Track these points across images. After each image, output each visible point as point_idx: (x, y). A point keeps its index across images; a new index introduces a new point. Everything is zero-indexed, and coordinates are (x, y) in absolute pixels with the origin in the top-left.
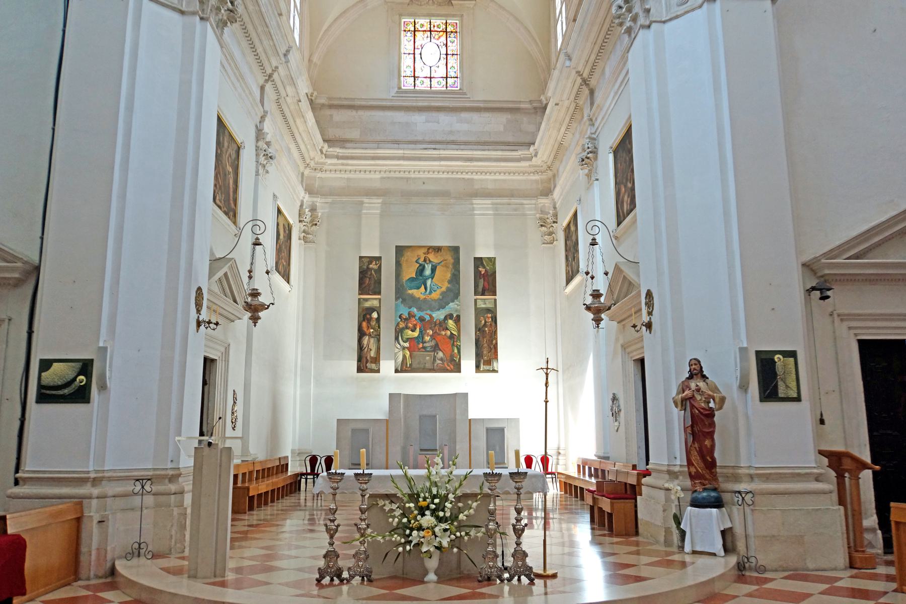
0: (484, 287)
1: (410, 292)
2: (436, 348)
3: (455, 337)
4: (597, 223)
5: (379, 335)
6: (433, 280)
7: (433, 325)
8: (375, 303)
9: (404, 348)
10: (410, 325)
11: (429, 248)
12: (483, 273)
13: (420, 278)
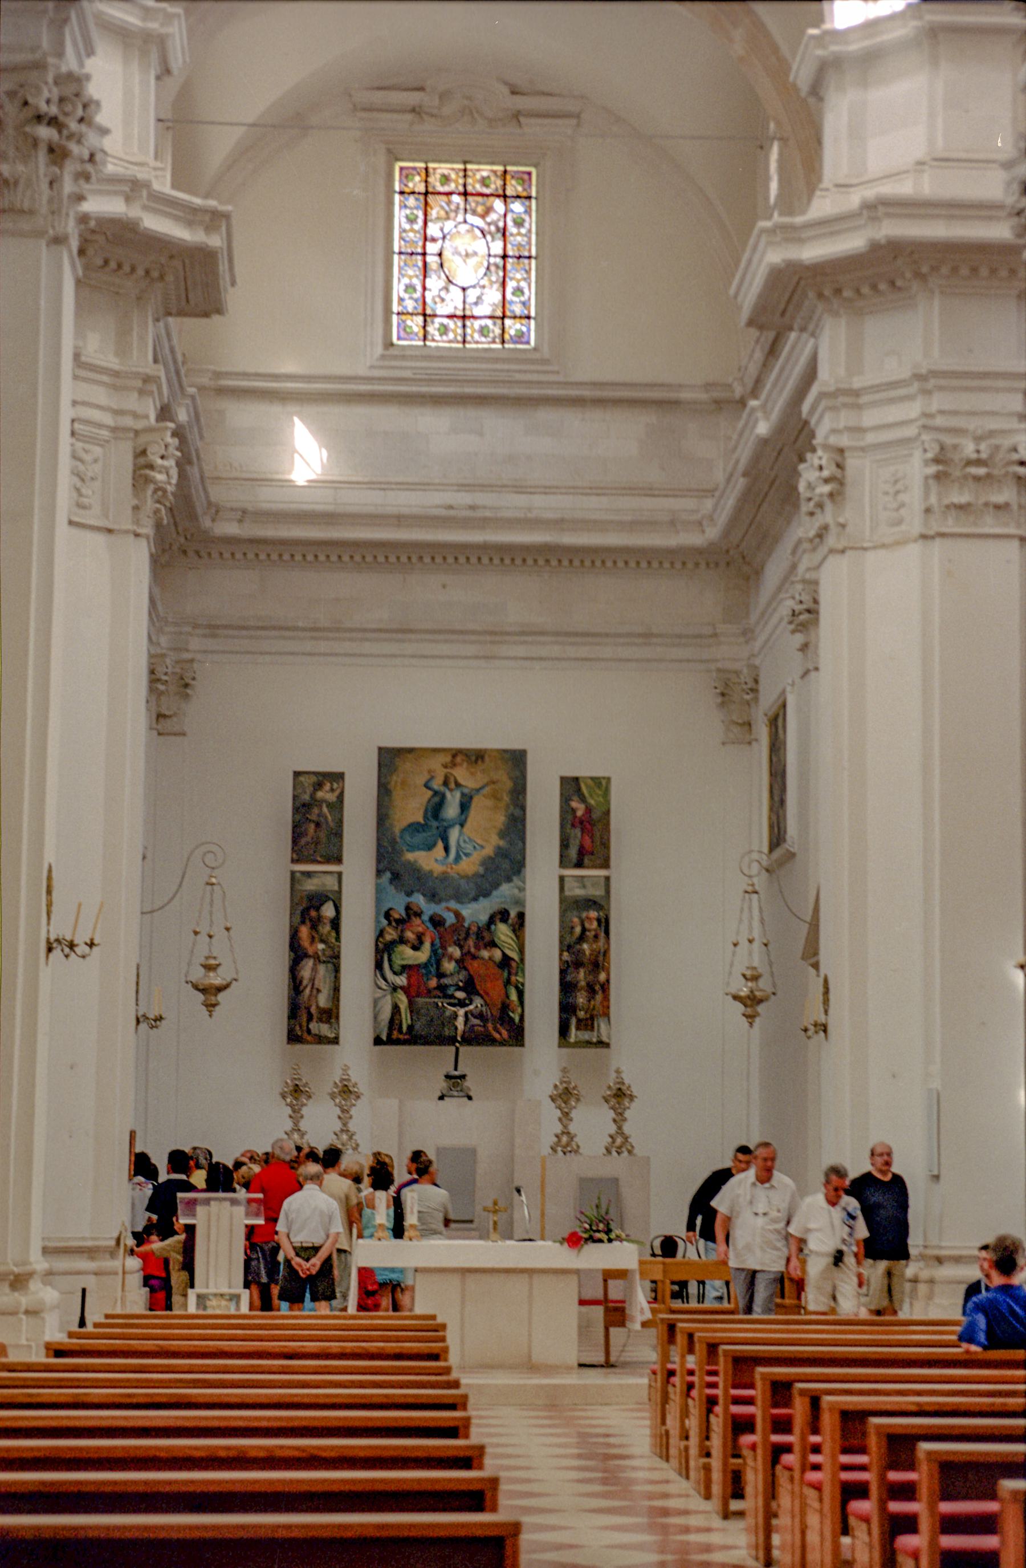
1: (410, 856)
3: (514, 964)
5: (338, 957)
6: (465, 830)
7: (463, 935)
8: (331, 883)
9: (395, 988)
10: (410, 935)
11: (456, 753)
12: (579, 813)
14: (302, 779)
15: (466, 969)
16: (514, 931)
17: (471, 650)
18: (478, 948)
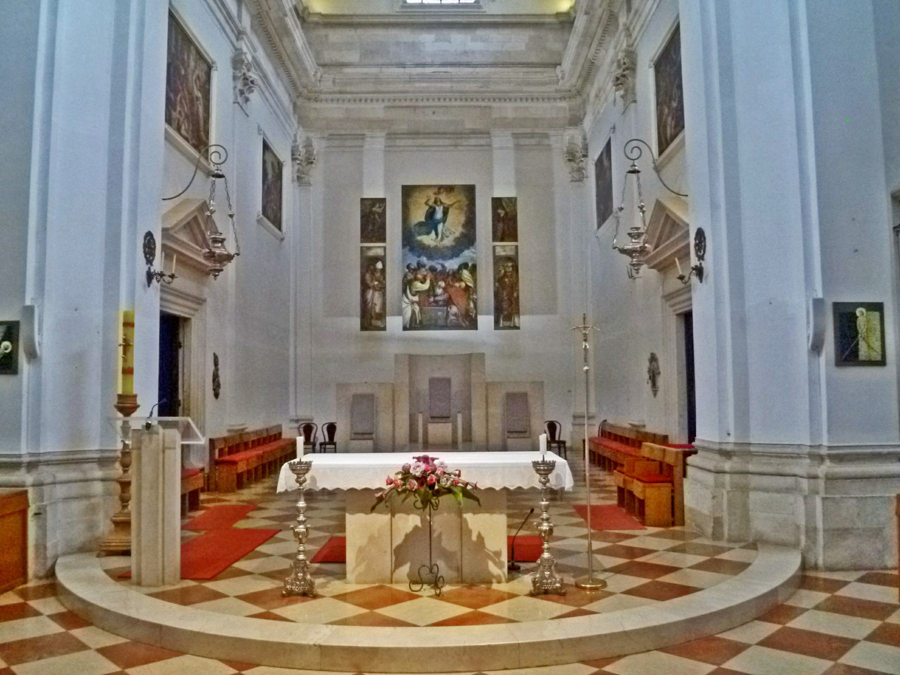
1: (419, 238)
2: (449, 302)
8: (380, 252)
9: (413, 303)
10: (419, 276)
11: (440, 188)
12: (502, 215)
13: (430, 224)
14: (365, 202)
15: (447, 292)
16: (471, 273)
17: (447, 142)
18: (452, 280)
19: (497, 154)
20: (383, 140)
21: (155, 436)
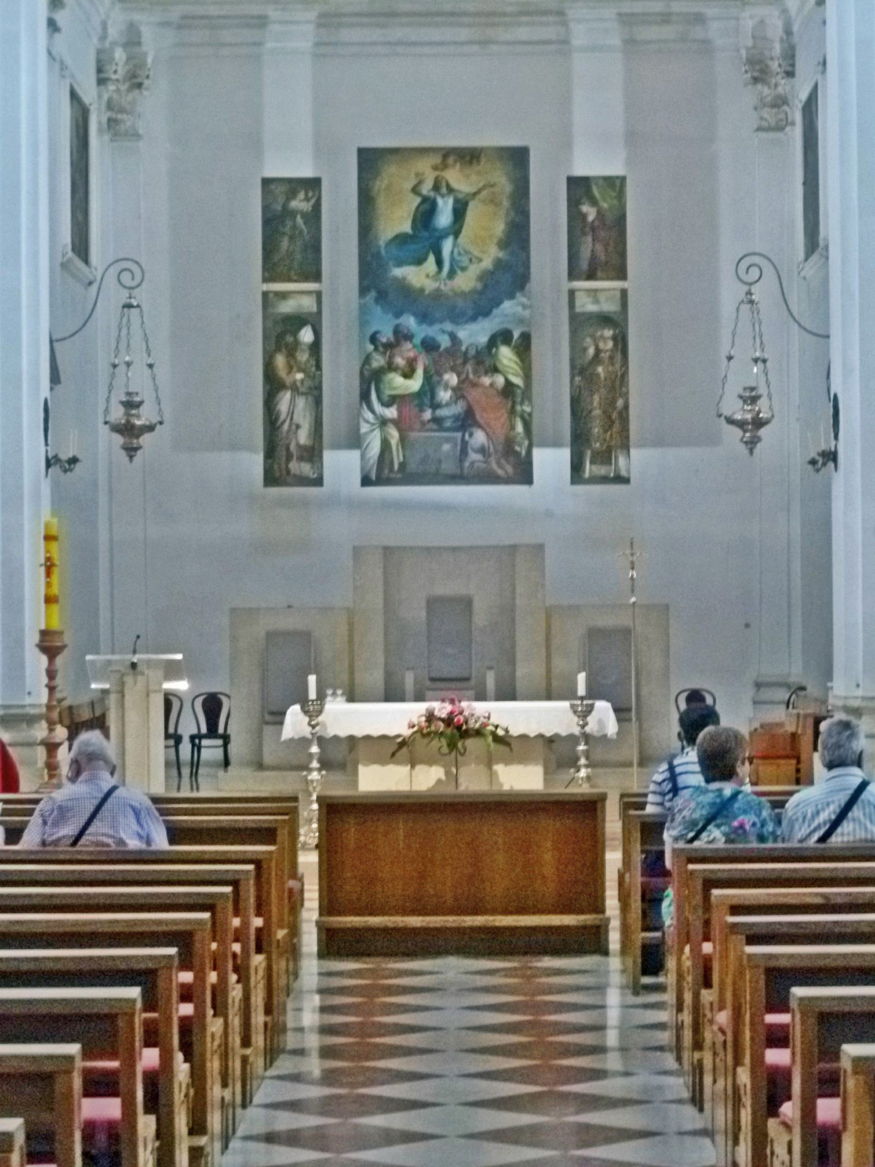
0: (593, 257)
1: (398, 272)
3: (519, 392)
4: (756, 260)
5: (319, 388)
7: (459, 361)
8: (308, 304)
9: (383, 422)
10: (400, 361)
12: (591, 218)
14: (272, 187)
15: (463, 397)
17: (464, 34)
18: (475, 372)
19: (581, 64)
20: (310, 28)
21: (139, 678)
